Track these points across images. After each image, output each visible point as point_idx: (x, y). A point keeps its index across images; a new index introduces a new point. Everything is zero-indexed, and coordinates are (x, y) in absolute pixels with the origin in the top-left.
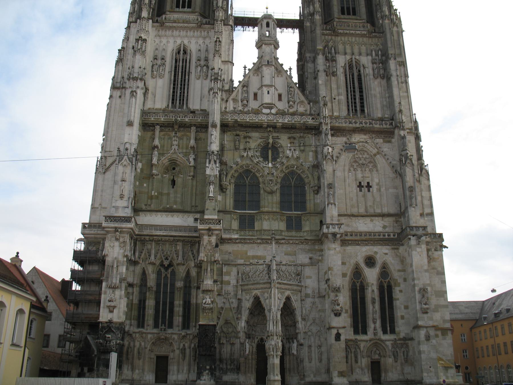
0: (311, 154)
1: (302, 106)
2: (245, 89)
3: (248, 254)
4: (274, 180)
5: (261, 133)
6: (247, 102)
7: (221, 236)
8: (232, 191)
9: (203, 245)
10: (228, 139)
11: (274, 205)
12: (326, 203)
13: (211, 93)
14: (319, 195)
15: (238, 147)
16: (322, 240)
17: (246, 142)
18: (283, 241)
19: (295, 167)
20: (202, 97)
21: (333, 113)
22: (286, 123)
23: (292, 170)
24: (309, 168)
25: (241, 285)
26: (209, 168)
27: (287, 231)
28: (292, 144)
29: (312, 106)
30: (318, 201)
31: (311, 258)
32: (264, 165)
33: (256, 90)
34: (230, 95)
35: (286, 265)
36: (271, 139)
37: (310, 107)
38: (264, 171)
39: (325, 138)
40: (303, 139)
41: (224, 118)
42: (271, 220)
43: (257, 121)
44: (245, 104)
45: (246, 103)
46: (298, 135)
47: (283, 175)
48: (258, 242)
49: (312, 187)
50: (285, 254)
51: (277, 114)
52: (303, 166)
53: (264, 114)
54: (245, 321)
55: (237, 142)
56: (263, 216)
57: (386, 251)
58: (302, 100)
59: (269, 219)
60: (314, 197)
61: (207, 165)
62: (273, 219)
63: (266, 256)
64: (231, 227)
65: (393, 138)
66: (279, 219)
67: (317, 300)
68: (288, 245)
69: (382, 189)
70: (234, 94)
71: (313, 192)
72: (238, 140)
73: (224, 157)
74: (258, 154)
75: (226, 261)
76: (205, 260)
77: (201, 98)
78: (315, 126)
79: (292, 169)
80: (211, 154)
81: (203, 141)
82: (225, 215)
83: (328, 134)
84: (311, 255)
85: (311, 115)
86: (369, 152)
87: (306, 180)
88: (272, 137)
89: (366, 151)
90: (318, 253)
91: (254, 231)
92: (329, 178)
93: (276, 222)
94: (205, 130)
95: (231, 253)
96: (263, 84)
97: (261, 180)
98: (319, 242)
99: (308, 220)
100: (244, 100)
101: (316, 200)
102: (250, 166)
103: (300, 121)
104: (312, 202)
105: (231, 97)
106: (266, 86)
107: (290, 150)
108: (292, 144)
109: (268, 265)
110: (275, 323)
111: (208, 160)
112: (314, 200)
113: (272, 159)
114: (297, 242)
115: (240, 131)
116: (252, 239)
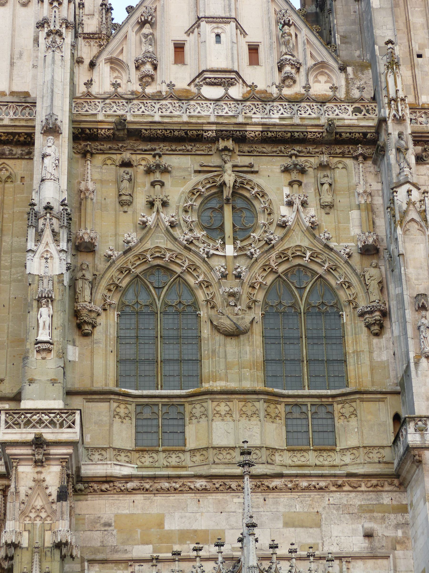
0: (355, 214)
1: (322, 79)
2: (147, 30)
3: (167, 527)
4: (244, 297)
5: (198, 158)
6: (155, 68)
7: (78, 469)
8: (113, 332)
9: (17, 493)
10: (97, 176)
11: (247, 372)
12: (412, 355)
13: (42, 34)
14: (387, 335)
15: (128, 198)
16: (404, 474)
17: (153, 184)
18: (276, 482)
19: (308, 254)
20: (16, 56)
21: (416, 97)
22: (274, 125)
23: (299, 265)
24: (350, 256)
26: (38, 255)
27: (289, 450)
28: (296, 186)
29: (351, 76)
30: (384, 357)
31: (368, 535)
32: (212, 252)
33: (180, 36)
34: (102, 48)
35: (289, 559)
36: (229, 172)
37: (347, 79)
38: (211, 269)
39: (398, 161)
40: (328, 172)
41: (83, 112)
42: (236, 415)
43: (185, 119)
44: (147, 76)
45: (152, 72)
46: (312, 160)
47: (270, 279)
48: (198, 485)
49: (362, 315)
50: (286, 525)
51: (245, 100)
52: (331, 249)
53: (207, 99)
55: (126, 184)
56: (210, 405)
58: (320, 60)
59: (229, 413)
60: (370, 344)
61: (31, 245)
62: (242, 413)
63: (223, 531)
64: (110, 440)
66: (262, 414)
68: (295, 495)
70: (114, 43)
71: (365, 329)
72: (127, 177)
73: (86, 229)
74: (193, 217)
75: (96, 550)
76: (25, 543)
77: (12, 58)
78: (364, 130)
79: (298, 261)
80: (42, 212)
81: (19, 182)
82: (90, 404)
83: (407, 149)
84: (369, 525)
85: (350, 101)
87: (343, 295)
88: (234, 166)
90: (392, 516)
91: (184, 451)
92: (417, 279)
93: (254, 421)
94: (26, 149)
95: (110, 525)
96: (201, 15)
97: (201, 296)
98: (391, 484)
99: (354, 414)
100: (144, 63)
101: (375, 354)
102: (168, 255)
103: (318, 118)
104: (365, 359)
105: (105, 55)
106: (211, 20)
107: (290, 204)
108: (296, 186)
109: (232, 558)
111: (32, 232)
112: (371, 352)
113: (234, 231)
114: (322, 484)
115: (135, 151)
116: (179, 477)
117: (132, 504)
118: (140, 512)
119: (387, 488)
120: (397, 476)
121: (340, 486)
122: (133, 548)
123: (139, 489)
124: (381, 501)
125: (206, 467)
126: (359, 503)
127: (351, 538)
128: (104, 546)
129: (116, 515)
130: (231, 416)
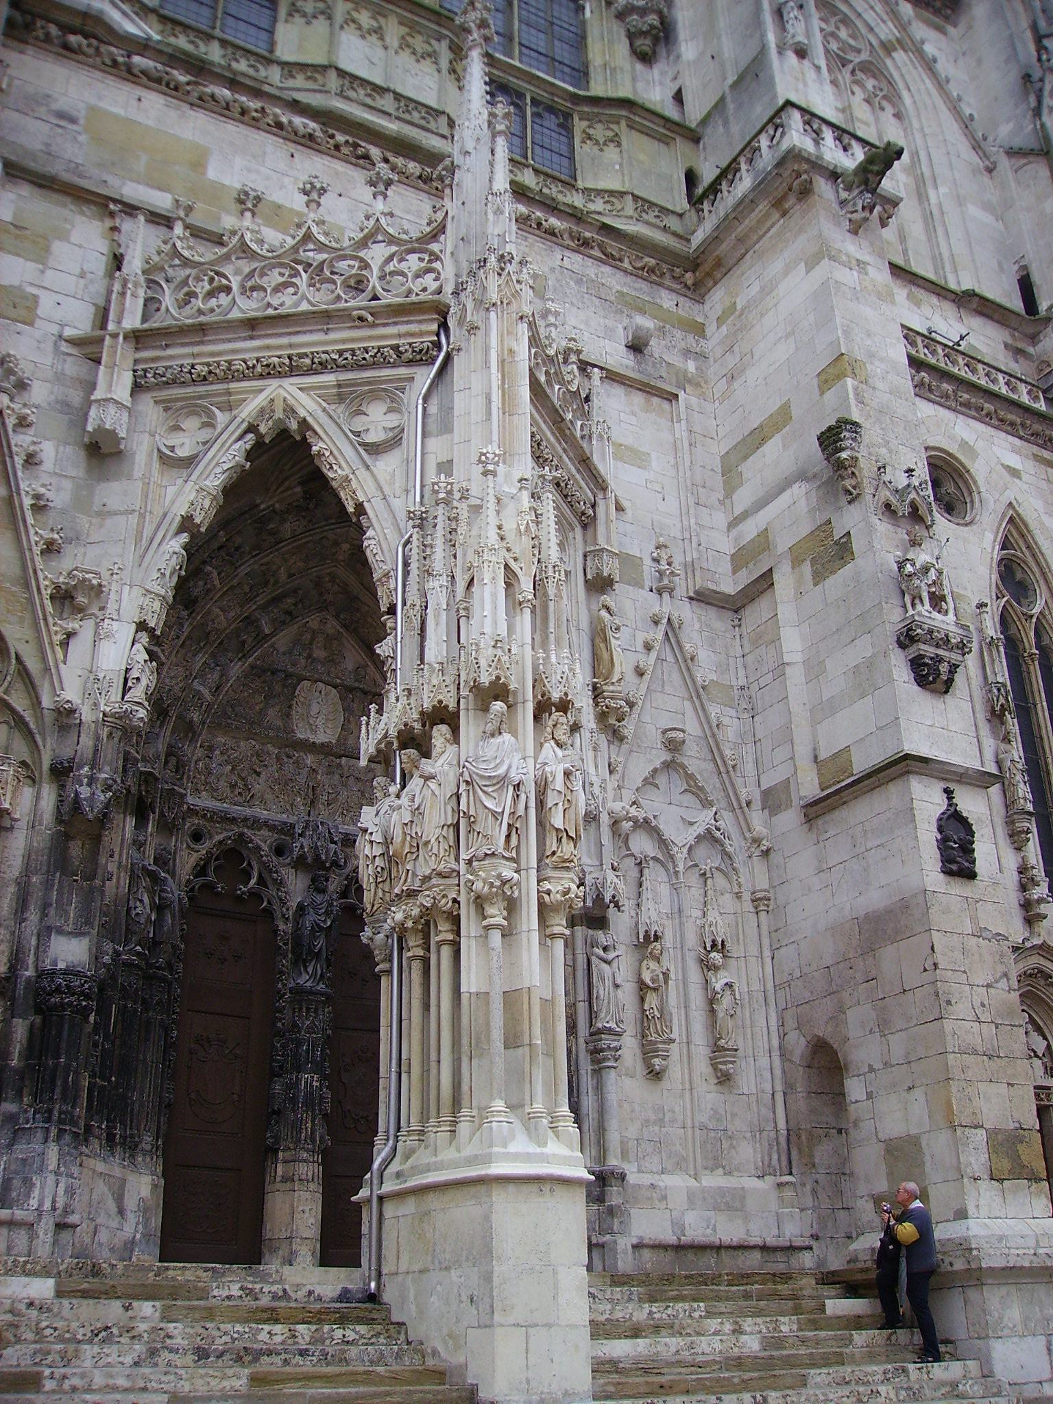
3: (212, 174)
25: (138, 338)
31: (637, 347)
54: (142, 626)
57: (1014, 461)
59: (378, 32)
65: (947, 18)
67: (686, 612)
69: (932, 194)
86: (859, 23)
89: (846, 21)
90: (678, 334)
93: (427, 66)
95: (73, 121)
99: (616, 140)
110: (526, 584)
117: (135, 103)
118: (151, 123)
119: (668, 281)
120: (693, 264)
121: (586, 243)
122: (124, 184)
123: (158, 81)
124: (658, 301)
125: (318, 96)
126: (619, 288)
127: (602, 342)
128: (49, 154)
129: (92, 109)
130: (382, 38)
